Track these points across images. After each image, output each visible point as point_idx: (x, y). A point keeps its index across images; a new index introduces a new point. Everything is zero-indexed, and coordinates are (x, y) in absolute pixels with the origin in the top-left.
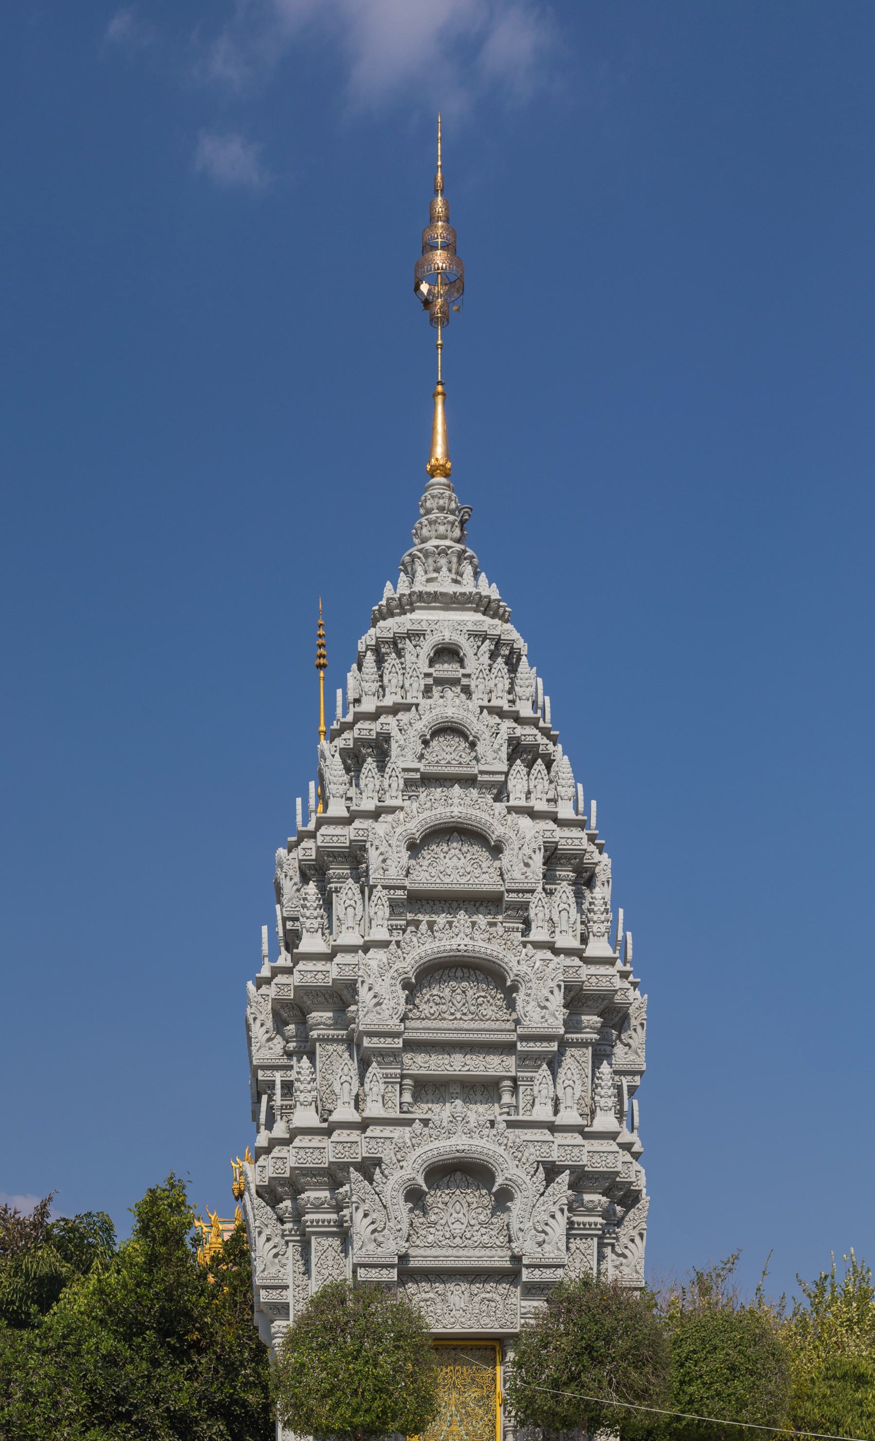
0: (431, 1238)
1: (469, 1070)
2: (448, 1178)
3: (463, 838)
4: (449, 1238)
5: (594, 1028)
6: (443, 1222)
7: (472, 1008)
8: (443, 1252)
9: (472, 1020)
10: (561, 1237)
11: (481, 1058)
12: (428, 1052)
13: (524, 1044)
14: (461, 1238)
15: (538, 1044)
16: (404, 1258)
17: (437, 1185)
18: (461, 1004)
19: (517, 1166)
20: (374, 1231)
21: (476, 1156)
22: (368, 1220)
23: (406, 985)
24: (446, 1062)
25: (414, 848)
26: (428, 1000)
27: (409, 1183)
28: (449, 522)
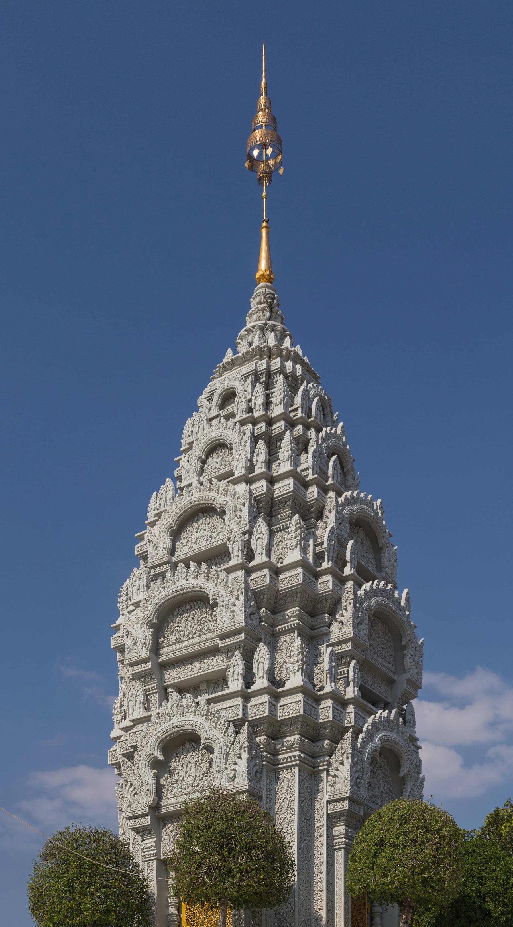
1: (203, 671)
2: (181, 747)
3: (205, 515)
4: (185, 789)
5: (294, 617)
6: (181, 778)
7: (199, 628)
9: (200, 636)
11: (211, 661)
12: (178, 667)
13: (223, 641)
14: (192, 786)
15: (232, 638)
17: (176, 754)
21: (185, 728)
22: (132, 788)
24: (190, 670)
26: (173, 631)
28: (260, 310)
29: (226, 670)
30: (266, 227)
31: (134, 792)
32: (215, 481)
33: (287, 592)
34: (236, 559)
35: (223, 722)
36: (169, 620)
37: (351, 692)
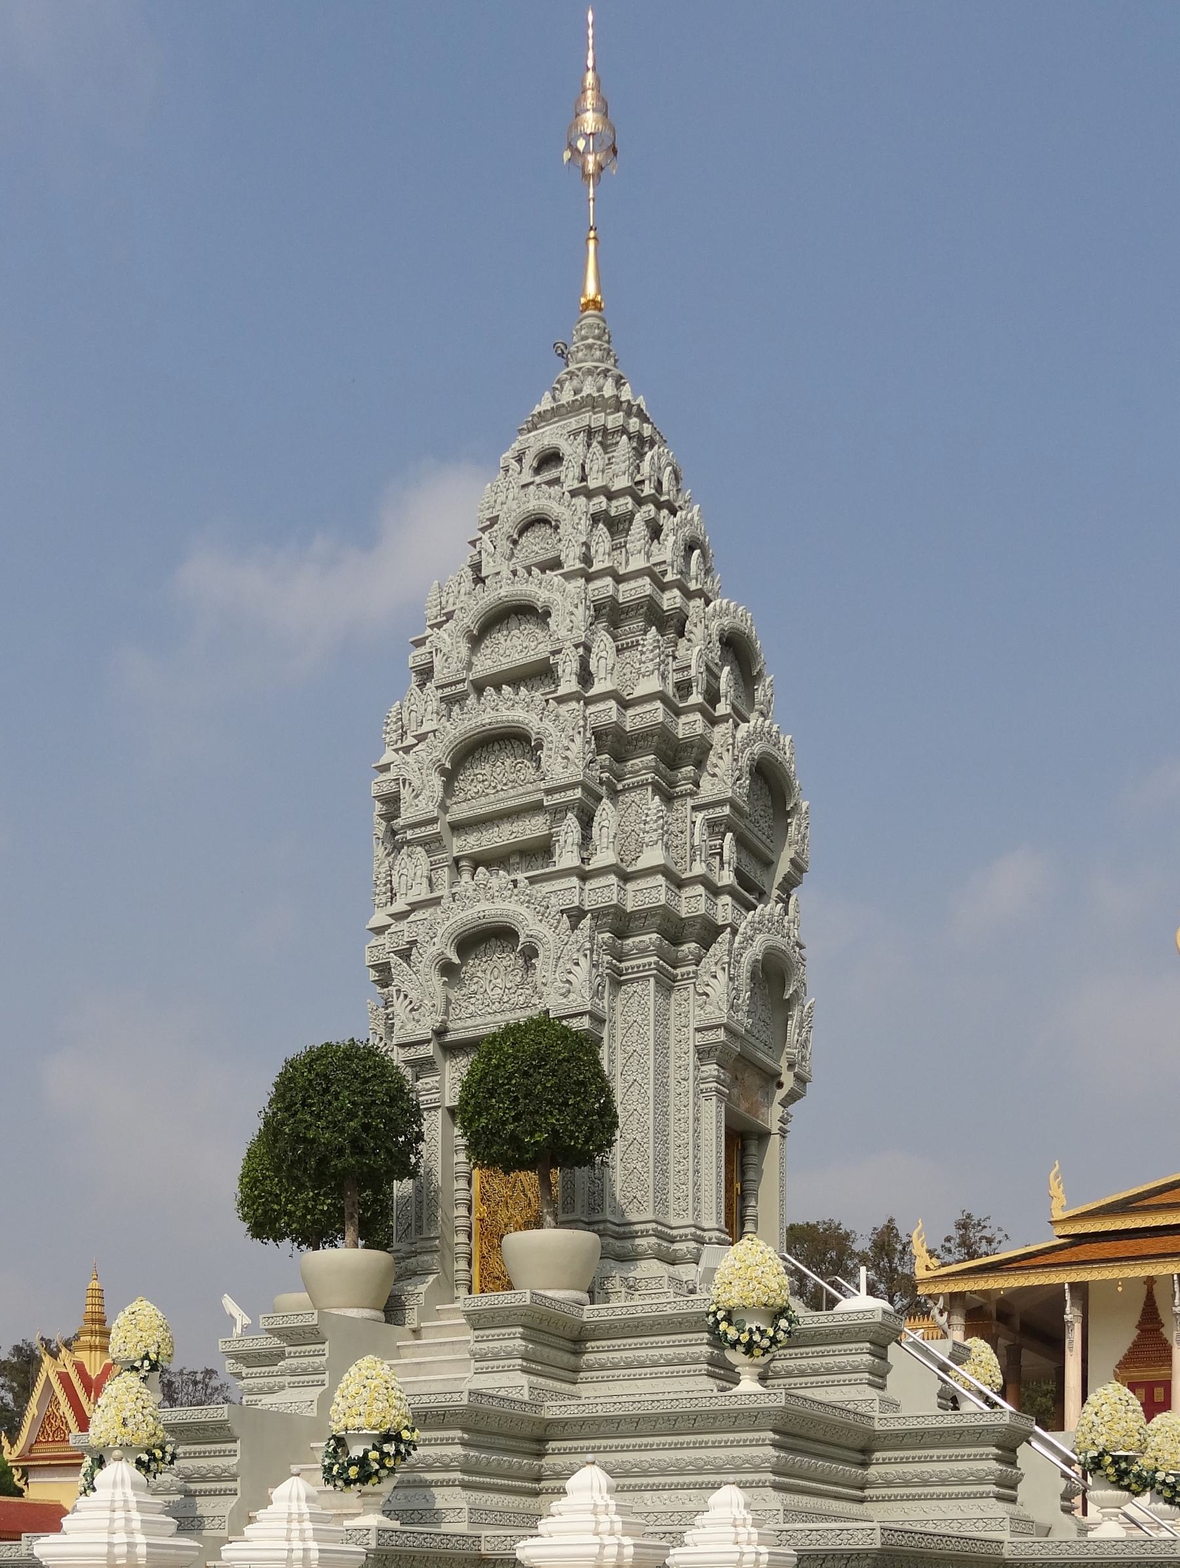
0: (472, 1008)
1: (516, 837)
2: (484, 945)
3: (520, 617)
4: (488, 1005)
6: (482, 990)
7: (512, 777)
8: (479, 1020)
9: (513, 787)
10: (584, 983)
14: (499, 1003)
16: (440, 1033)
17: (476, 955)
18: (501, 775)
19: (541, 921)
20: (412, 1010)
22: (408, 1001)
23: (443, 772)
24: (496, 834)
25: (476, 640)
27: (440, 958)
29: (551, 835)
30: (595, 238)
31: (410, 1007)
32: (535, 571)
33: (639, 734)
34: (568, 684)
35: (553, 913)
36: (468, 765)
37: (727, 878)
